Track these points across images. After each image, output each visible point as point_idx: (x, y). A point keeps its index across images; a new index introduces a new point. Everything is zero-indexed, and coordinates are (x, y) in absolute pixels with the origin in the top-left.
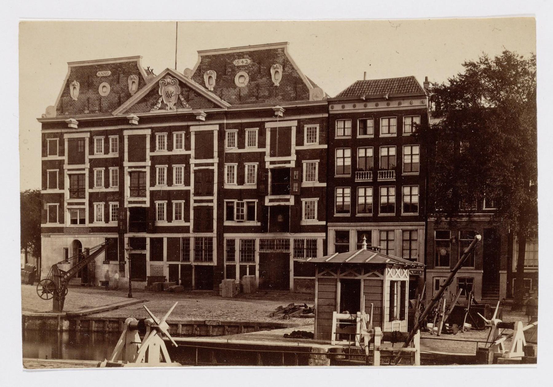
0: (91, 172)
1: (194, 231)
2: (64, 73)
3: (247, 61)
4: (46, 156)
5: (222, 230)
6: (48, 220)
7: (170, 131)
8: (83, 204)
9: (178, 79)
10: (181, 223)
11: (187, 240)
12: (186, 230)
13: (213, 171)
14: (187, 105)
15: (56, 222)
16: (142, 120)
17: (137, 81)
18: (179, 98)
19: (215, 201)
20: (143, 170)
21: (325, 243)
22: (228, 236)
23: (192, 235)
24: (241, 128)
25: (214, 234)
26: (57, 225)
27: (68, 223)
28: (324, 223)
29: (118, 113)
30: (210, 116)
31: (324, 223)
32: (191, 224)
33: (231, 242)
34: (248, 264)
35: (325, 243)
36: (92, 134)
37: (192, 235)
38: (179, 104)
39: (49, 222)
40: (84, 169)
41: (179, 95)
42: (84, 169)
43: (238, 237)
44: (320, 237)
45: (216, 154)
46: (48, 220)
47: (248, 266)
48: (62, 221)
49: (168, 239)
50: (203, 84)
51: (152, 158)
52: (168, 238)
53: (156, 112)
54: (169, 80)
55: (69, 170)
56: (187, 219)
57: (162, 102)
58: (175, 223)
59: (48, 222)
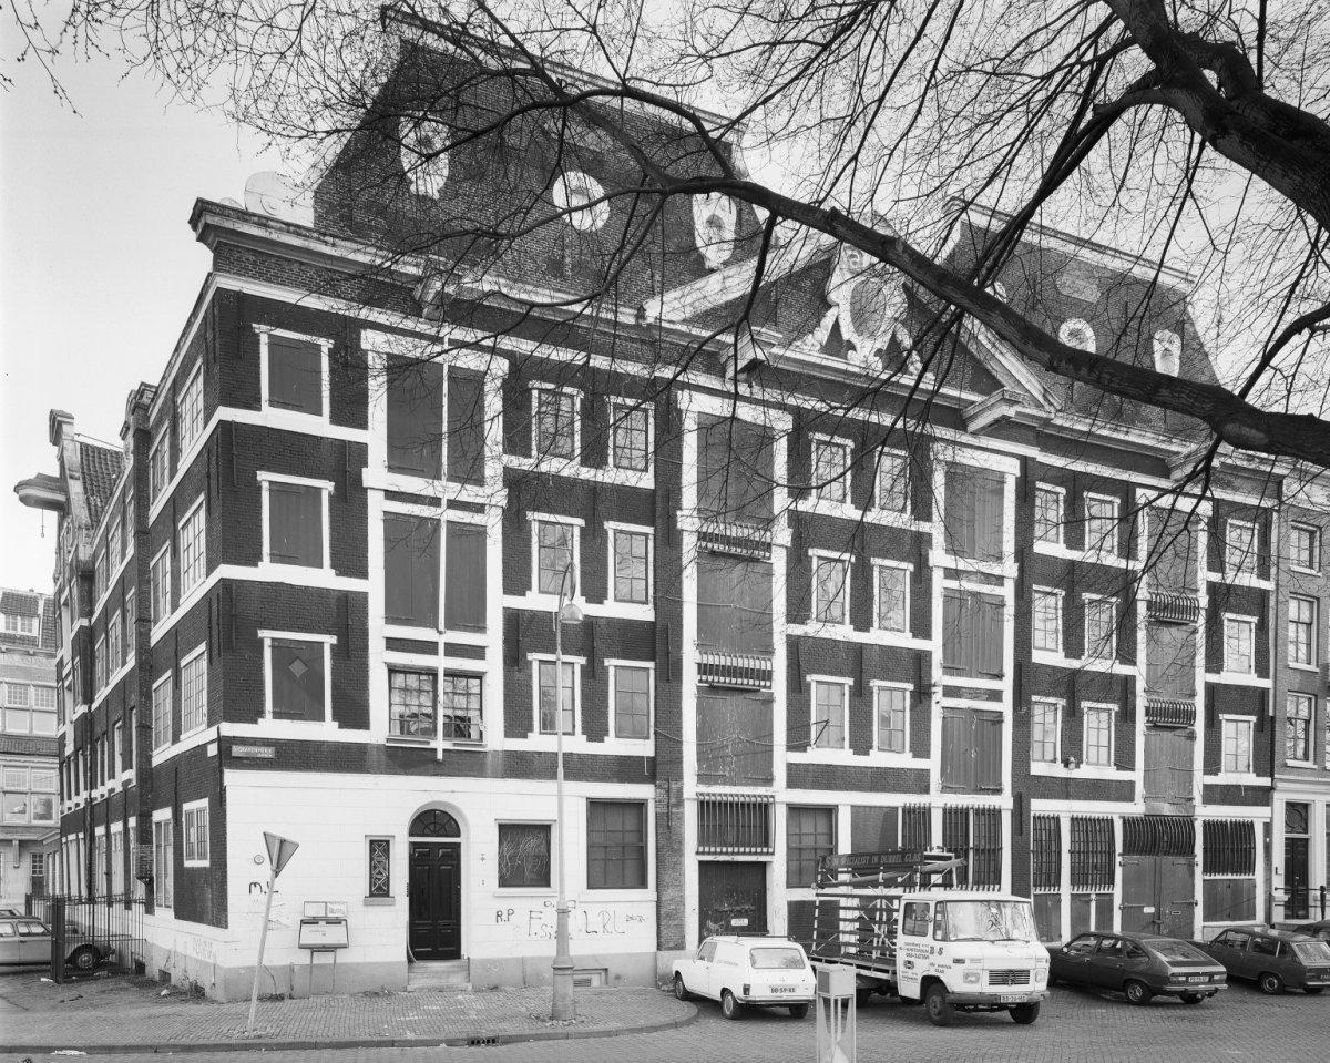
1: (945, 789)
5: (1028, 787)
6: (269, 705)
8: (478, 652)
10: (906, 761)
11: (919, 817)
12: (920, 782)
15: (320, 717)
18: (894, 335)
19: (1008, 696)
21: (1268, 828)
22: (1039, 806)
25: (1004, 802)
26: (326, 730)
27: (378, 731)
28: (1265, 781)
31: (1265, 781)
32: (933, 764)
34: (1093, 893)
35: (1268, 828)
37: (938, 800)
38: (894, 356)
39: (277, 715)
44: (1255, 814)
45: (1009, 545)
46: (269, 705)
47: (1093, 897)
48: (353, 711)
49: (857, 810)
52: (857, 810)
57: (836, 326)
58: (877, 759)
59: (269, 715)
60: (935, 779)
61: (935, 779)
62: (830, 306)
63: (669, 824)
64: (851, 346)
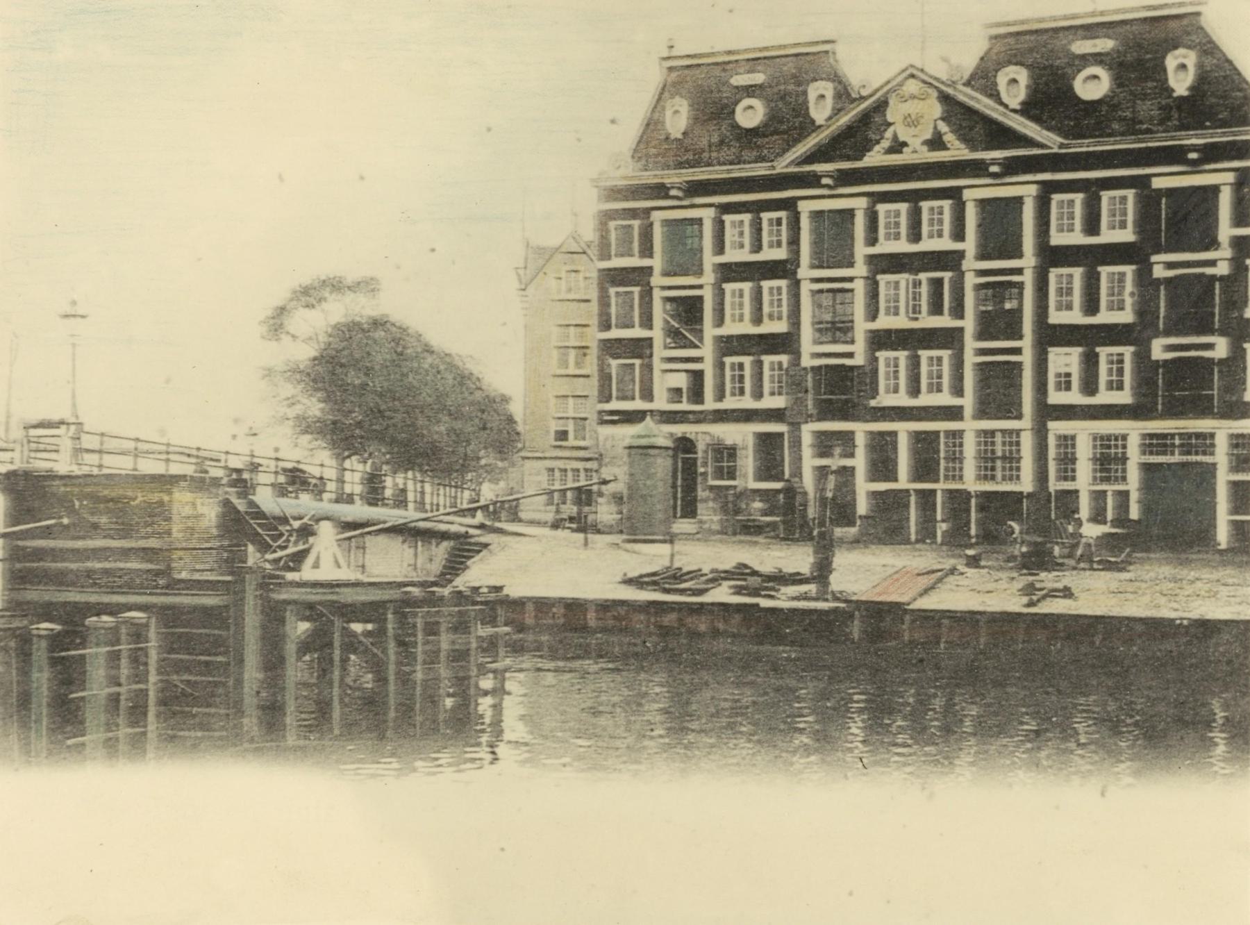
0: (720, 294)
2: (655, 77)
3: (1105, 45)
4: (609, 258)
7: (914, 197)
9: (936, 87)
10: (945, 399)
11: (957, 435)
12: (954, 413)
13: (1020, 286)
14: (957, 143)
16: (845, 178)
17: (829, 94)
18: (935, 127)
20: (847, 285)
22: (1057, 427)
23: (970, 426)
24: (1092, 190)
25: (1026, 423)
29: (783, 165)
30: (1012, 167)
32: (968, 402)
33: (1067, 441)
34: (1110, 488)
36: (1048, 189)
38: (936, 143)
40: (700, 287)
41: (936, 120)
42: (700, 287)
43: (1084, 432)
48: (648, 395)
50: (996, 96)
51: (871, 259)
53: (875, 158)
54: (912, 87)
55: (664, 288)
56: (958, 391)
58: (926, 400)
60: (968, 412)
61: (968, 412)
62: (890, 124)
63: (797, 444)
64: (905, 144)
